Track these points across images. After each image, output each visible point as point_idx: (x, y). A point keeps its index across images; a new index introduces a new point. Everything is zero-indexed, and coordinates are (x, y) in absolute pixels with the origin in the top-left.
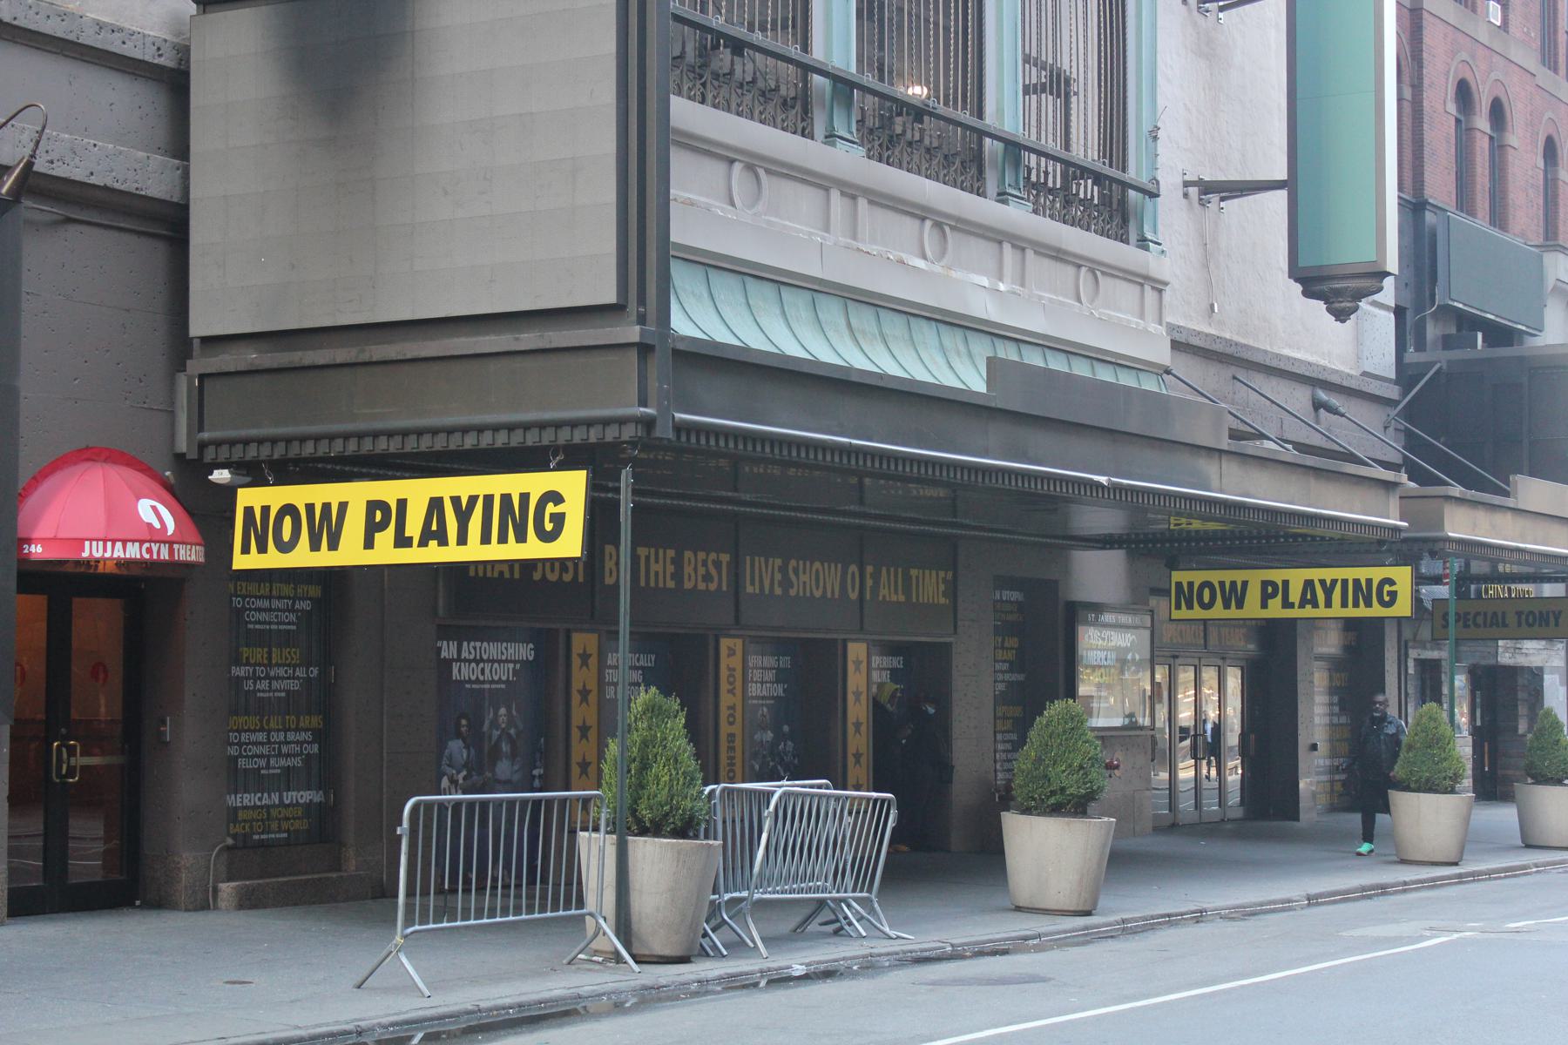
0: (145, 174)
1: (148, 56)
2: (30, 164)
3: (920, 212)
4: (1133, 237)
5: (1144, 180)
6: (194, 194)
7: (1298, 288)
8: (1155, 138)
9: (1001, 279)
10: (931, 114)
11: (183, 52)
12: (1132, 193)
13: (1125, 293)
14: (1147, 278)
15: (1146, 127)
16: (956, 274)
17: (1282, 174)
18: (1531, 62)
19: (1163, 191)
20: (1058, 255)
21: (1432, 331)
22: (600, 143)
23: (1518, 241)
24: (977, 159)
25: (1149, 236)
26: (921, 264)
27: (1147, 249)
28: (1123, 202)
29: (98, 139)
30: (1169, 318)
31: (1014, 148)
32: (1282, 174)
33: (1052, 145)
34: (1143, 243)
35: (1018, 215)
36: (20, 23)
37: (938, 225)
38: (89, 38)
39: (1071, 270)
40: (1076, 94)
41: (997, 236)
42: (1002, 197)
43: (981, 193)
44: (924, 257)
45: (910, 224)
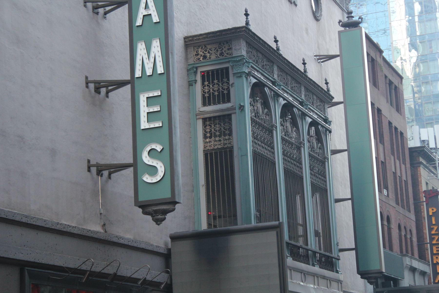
0: (162, 278)
1: (162, 251)
2: (167, 282)
3: (301, 271)
4: (335, 270)
5: (336, 256)
6: (173, 282)
7: (360, 276)
8: (338, 245)
9: (315, 285)
10: (302, 248)
11: (169, 250)
12: (334, 259)
13: (334, 284)
14: (339, 280)
15: (336, 243)
16: (308, 285)
17: (354, 247)
18: (393, 203)
19: (341, 258)
20: (324, 277)
21: (380, 281)
22: (276, 271)
23: (396, 254)
24: (307, 256)
25: (338, 270)
26: (302, 283)
27: (338, 273)
28: (332, 262)
29: (147, 270)
30: (343, 289)
31: (315, 253)
32: (354, 247)
33: (317, 250)
34: (337, 272)
35: (317, 269)
36: (147, 248)
37: (304, 274)
38: (155, 250)
39: (326, 281)
40: (317, 234)
41: (314, 275)
42: (313, 265)
43: (309, 265)
44: (302, 282)
45: (299, 274)
